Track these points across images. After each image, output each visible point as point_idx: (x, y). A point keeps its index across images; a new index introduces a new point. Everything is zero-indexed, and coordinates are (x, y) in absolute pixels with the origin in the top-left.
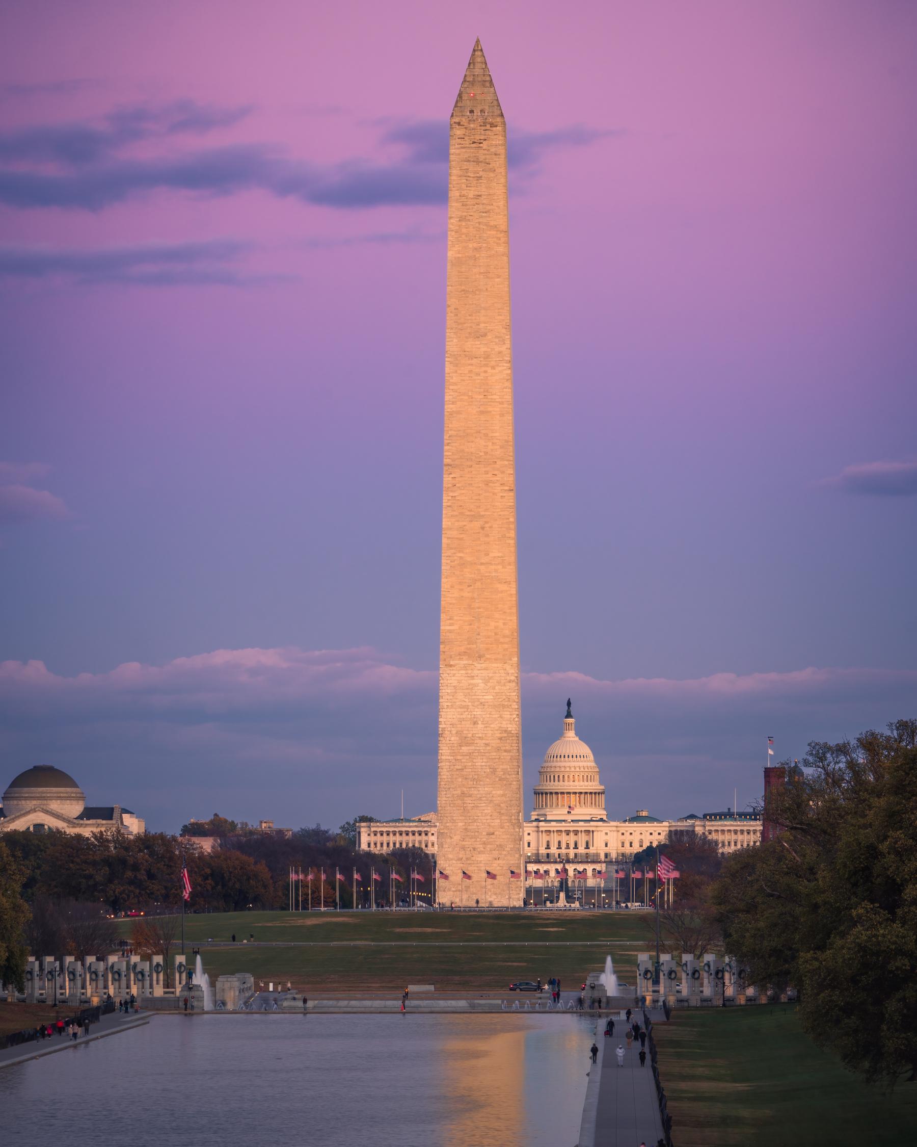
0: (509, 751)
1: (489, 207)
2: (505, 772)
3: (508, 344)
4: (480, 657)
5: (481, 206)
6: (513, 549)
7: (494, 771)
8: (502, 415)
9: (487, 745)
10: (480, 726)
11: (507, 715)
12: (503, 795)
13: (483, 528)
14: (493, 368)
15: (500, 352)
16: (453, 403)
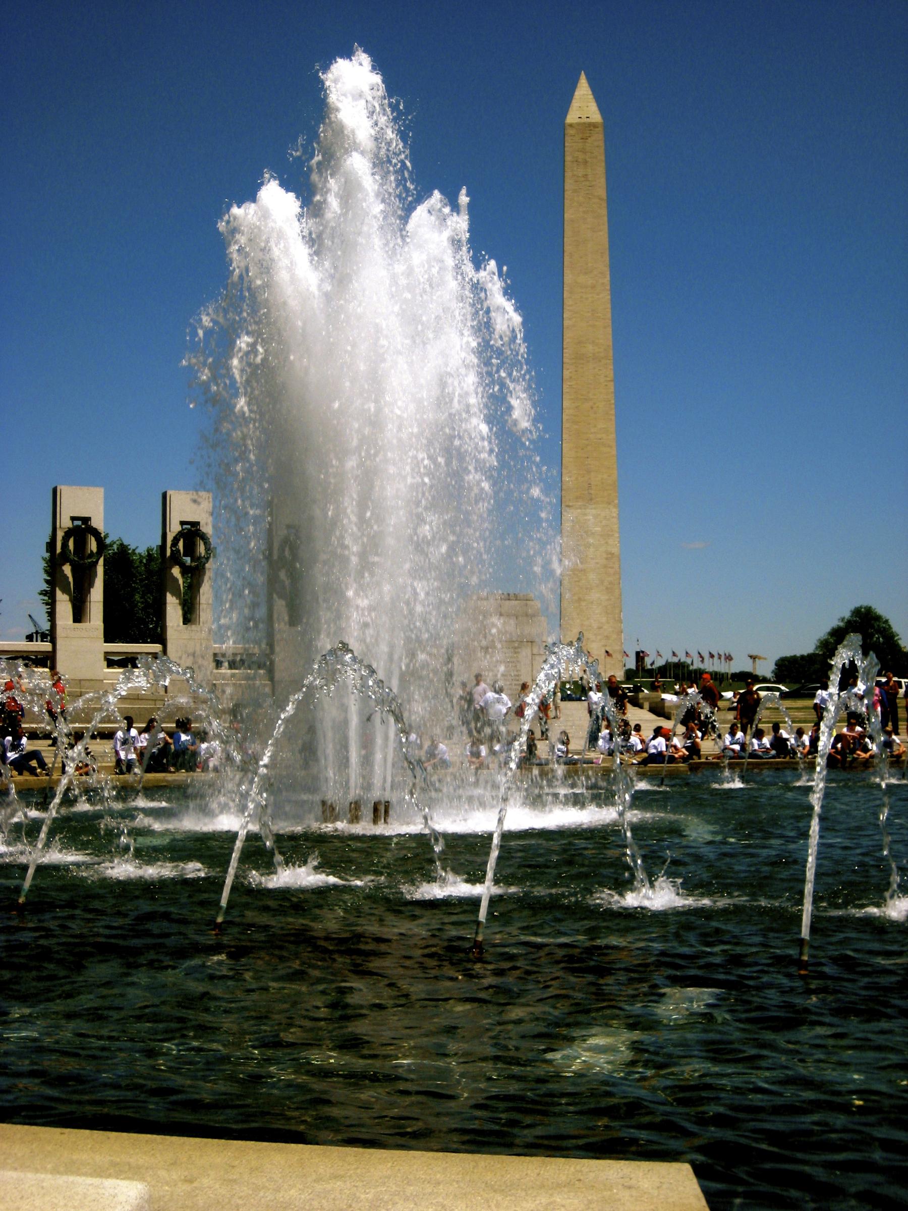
0: (612, 568)
1: (594, 183)
2: (611, 583)
3: (608, 278)
4: (591, 499)
5: (587, 183)
6: (614, 422)
7: (602, 582)
8: (605, 327)
9: (597, 563)
10: (592, 550)
11: (610, 541)
12: (609, 600)
13: (592, 408)
14: (598, 294)
15: (603, 284)
16: (570, 319)
